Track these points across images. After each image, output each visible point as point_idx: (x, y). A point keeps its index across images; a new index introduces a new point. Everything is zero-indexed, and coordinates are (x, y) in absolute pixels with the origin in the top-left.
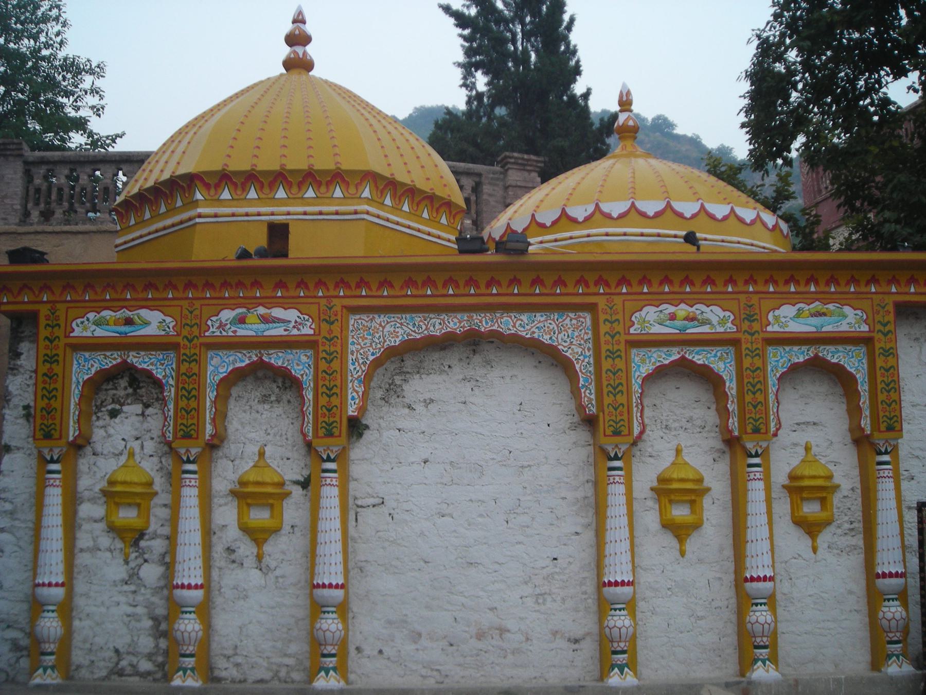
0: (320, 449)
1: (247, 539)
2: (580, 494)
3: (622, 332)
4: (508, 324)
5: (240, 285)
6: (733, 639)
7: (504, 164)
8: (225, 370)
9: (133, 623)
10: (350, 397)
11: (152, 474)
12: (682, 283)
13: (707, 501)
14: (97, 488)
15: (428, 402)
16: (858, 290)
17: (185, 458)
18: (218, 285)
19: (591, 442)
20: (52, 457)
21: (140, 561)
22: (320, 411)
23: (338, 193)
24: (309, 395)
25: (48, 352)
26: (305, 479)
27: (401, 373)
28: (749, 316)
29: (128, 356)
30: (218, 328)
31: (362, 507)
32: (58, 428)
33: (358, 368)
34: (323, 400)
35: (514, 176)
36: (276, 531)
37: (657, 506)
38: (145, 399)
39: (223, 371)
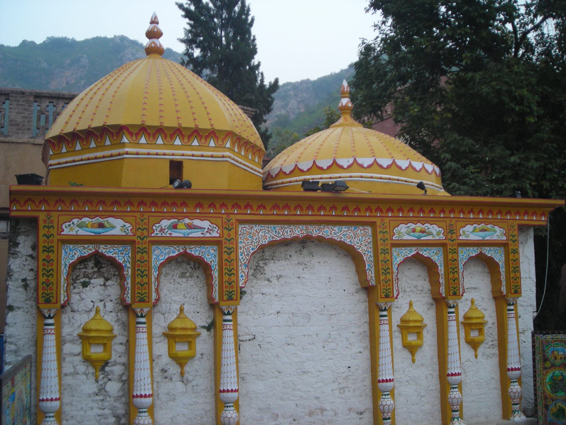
0: (224, 308)
1: (174, 363)
2: (361, 330)
3: (389, 239)
4: (328, 232)
5: (174, 204)
6: (438, 407)
8: (163, 258)
9: (103, 420)
10: (240, 275)
11: (112, 323)
12: (419, 212)
13: (425, 332)
14: (75, 334)
15: (279, 277)
16: (502, 217)
17: (140, 315)
18: (159, 204)
19: (367, 300)
20: (50, 315)
21: (106, 380)
22: (224, 285)
23: (212, 144)
25: (46, 244)
26: (209, 325)
27: (263, 259)
28: (451, 231)
29: (100, 248)
30: (160, 231)
31: (242, 341)
32: (55, 296)
33: (244, 258)
34: (226, 278)
36: (192, 357)
37: (400, 335)
38: (106, 275)
39: (162, 259)
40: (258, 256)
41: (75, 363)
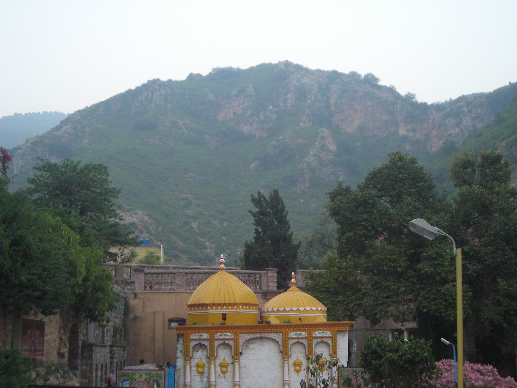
4: (267, 335)
7: (267, 270)
15: (253, 349)
23: (235, 307)
24: (233, 348)
28: (310, 334)
35: (270, 274)
39: (218, 344)
40: (247, 342)
41: (195, 373)
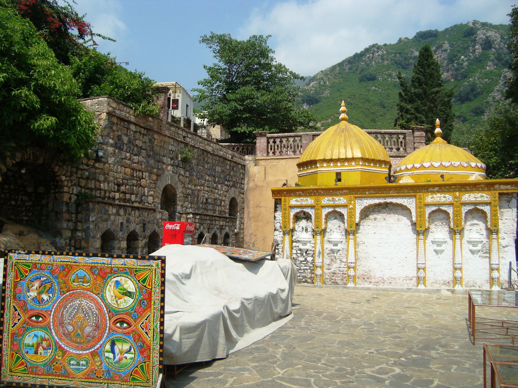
15: (375, 219)
